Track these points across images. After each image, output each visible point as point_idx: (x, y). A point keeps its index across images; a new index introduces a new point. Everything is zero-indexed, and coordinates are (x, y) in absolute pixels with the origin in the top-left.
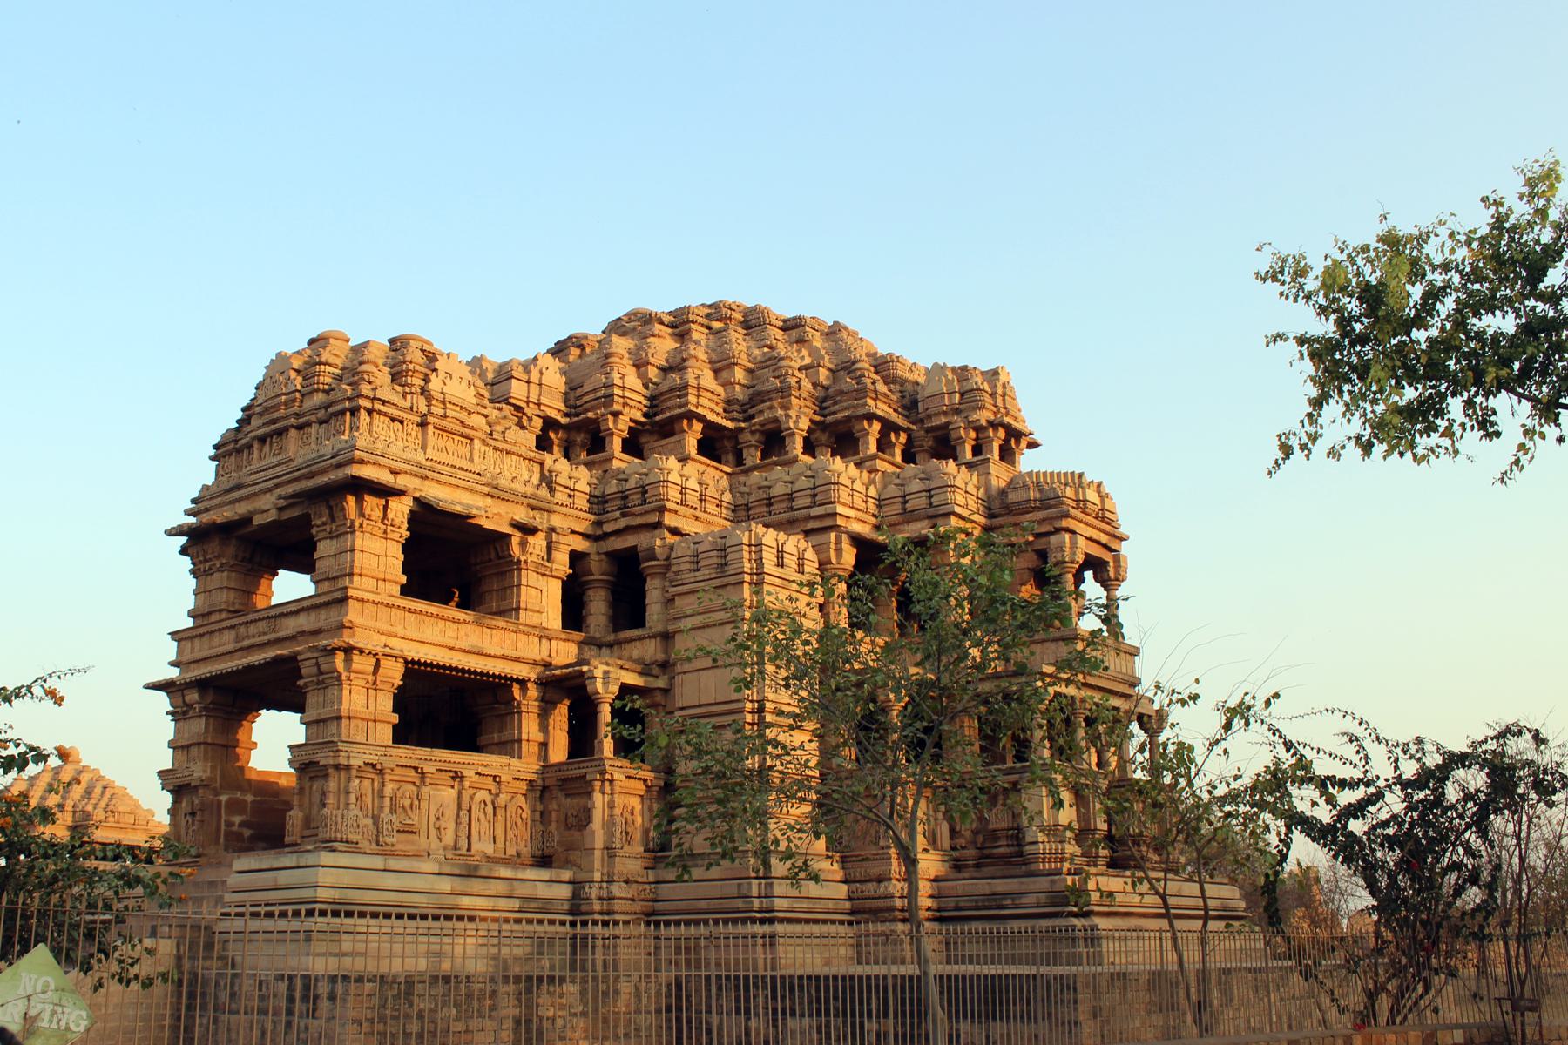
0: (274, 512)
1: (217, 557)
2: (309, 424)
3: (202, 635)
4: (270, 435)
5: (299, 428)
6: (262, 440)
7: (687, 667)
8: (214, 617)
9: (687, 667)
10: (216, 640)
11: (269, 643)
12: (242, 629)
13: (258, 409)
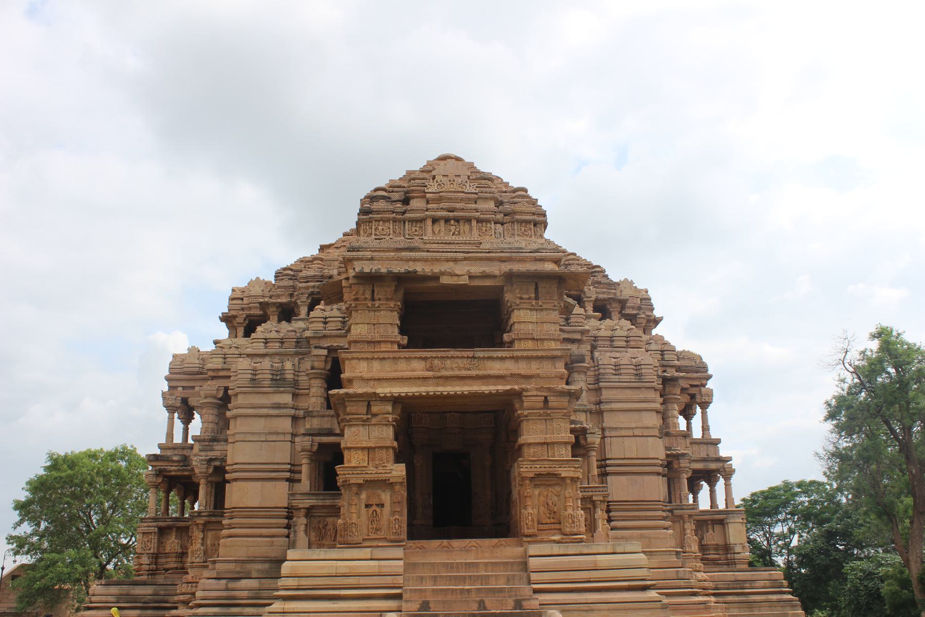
0: (467, 277)
1: (387, 299)
2: (488, 221)
4: (447, 220)
5: (479, 221)
6: (435, 221)
7: (613, 433)
8: (384, 347)
9: (613, 433)
10: (402, 365)
12: (436, 362)
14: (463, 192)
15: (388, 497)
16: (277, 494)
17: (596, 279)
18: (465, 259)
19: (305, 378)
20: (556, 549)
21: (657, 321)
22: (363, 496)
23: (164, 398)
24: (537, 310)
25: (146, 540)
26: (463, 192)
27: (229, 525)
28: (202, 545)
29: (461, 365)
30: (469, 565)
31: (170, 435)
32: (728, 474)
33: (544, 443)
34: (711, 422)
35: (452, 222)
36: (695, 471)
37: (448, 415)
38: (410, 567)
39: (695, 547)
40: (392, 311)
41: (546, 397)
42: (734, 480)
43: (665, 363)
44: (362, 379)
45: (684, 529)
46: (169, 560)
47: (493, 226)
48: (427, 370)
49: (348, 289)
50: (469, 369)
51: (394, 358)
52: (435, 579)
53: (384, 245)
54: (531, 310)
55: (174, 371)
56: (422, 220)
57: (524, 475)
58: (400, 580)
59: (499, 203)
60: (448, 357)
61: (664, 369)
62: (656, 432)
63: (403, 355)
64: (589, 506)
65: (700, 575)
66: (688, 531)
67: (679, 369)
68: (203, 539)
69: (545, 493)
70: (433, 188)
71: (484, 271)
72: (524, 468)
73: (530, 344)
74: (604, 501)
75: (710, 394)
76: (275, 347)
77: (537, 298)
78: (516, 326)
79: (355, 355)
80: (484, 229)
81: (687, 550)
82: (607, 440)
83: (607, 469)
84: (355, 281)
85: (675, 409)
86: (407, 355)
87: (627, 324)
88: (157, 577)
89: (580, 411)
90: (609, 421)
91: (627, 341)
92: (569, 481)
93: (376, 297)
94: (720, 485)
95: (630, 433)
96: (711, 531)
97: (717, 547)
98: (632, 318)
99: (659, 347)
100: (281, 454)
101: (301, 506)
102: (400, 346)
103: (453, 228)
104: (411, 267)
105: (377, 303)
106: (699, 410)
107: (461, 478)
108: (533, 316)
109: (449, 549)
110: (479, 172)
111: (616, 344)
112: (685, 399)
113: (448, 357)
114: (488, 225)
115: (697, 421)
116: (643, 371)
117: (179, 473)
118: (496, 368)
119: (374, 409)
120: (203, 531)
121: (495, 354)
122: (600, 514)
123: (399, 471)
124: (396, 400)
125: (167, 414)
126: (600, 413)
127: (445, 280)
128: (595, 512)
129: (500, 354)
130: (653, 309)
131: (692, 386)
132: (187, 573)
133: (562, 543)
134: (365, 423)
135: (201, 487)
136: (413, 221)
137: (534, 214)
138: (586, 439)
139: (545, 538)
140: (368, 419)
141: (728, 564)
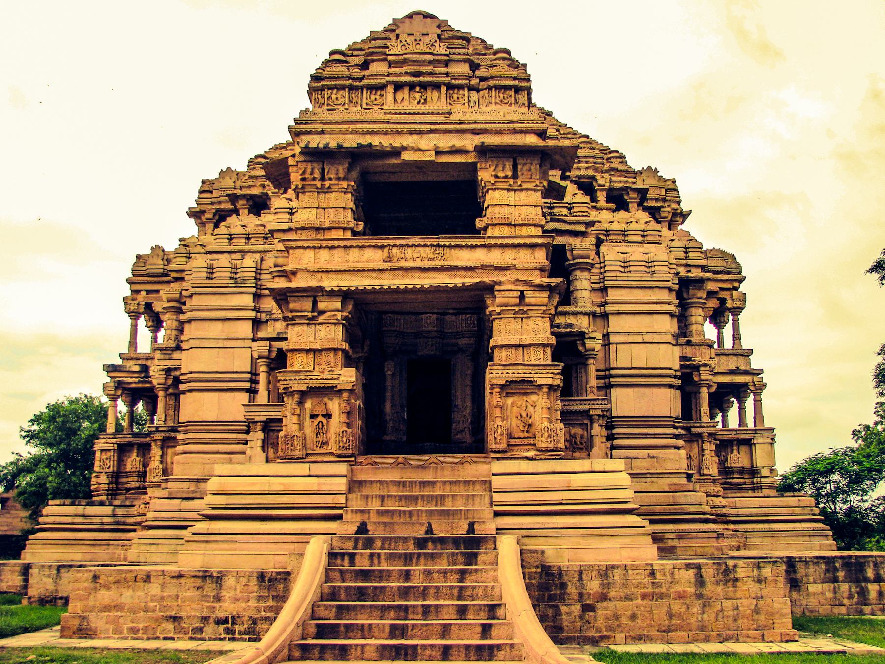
1: (339, 179)
2: (460, 87)
3: (332, 248)
4: (412, 86)
5: (450, 87)
6: (398, 87)
8: (335, 234)
10: (354, 254)
11: (443, 269)
13: (390, 58)
14: (431, 54)
15: (336, 406)
16: (234, 406)
17: (612, 165)
18: (432, 131)
19: (269, 276)
20: (524, 466)
21: (685, 216)
22: (308, 405)
23: (126, 303)
24: (515, 190)
25: (104, 457)
26: (431, 54)
27: (184, 440)
28: (161, 462)
29: (424, 255)
30: (423, 484)
31: (133, 343)
32: (760, 388)
33: (519, 346)
34: (742, 331)
35: (418, 89)
36: (720, 385)
37: (424, 316)
38: (354, 485)
39: (714, 470)
40: (345, 193)
41: (522, 292)
42: (765, 396)
43: (690, 262)
44: (308, 271)
45: (703, 450)
46: (130, 479)
47: (466, 93)
48: (384, 261)
49: (295, 169)
50: (433, 259)
51: (345, 247)
52: (382, 498)
53: (334, 116)
54: (508, 190)
55: (136, 273)
56: (382, 87)
57: (494, 381)
58: (341, 499)
59: (474, 67)
60: (408, 246)
61: (689, 268)
62: (669, 338)
63: (355, 243)
64: (585, 421)
65: (717, 501)
66: (706, 452)
67: (704, 268)
68: (162, 456)
69: (519, 403)
70: (396, 49)
71: (454, 146)
72: (494, 375)
73: (506, 231)
74: (603, 416)
75: (743, 298)
76: (240, 244)
77: (515, 176)
78: (490, 210)
79: (300, 244)
80: (455, 96)
81: (705, 472)
82: (612, 348)
83: (611, 380)
84: (302, 158)
85: (697, 315)
86: (361, 243)
87: (643, 216)
88: (117, 497)
89: (581, 313)
90: (615, 325)
91: (643, 236)
92: (545, 390)
93: (326, 176)
94: (750, 403)
95: (639, 339)
96: (735, 452)
97: (742, 471)
98: (654, 212)
99: (683, 243)
100: (240, 362)
101: (257, 419)
102: (354, 233)
103: (418, 96)
104: (365, 140)
105: (327, 184)
106: (731, 317)
107: (417, 382)
108: (513, 198)
109: (405, 463)
110: (453, 30)
111: (631, 238)
112: (713, 304)
113: (408, 246)
114: (461, 92)
115: (728, 331)
116: (656, 268)
117: (140, 385)
118: (464, 258)
119: (321, 306)
120: (162, 448)
121: (463, 242)
122: (598, 430)
123: (348, 377)
124: (345, 295)
125: (127, 321)
126: (605, 316)
127: (407, 156)
128: (592, 428)
129: (469, 242)
130: (679, 203)
131: (722, 289)
132: (146, 493)
133: (536, 460)
134: (312, 321)
135: (160, 399)
136: (372, 88)
137: (515, 78)
138: (584, 345)
139: (517, 454)
140: (313, 316)
141: (753, 490)
